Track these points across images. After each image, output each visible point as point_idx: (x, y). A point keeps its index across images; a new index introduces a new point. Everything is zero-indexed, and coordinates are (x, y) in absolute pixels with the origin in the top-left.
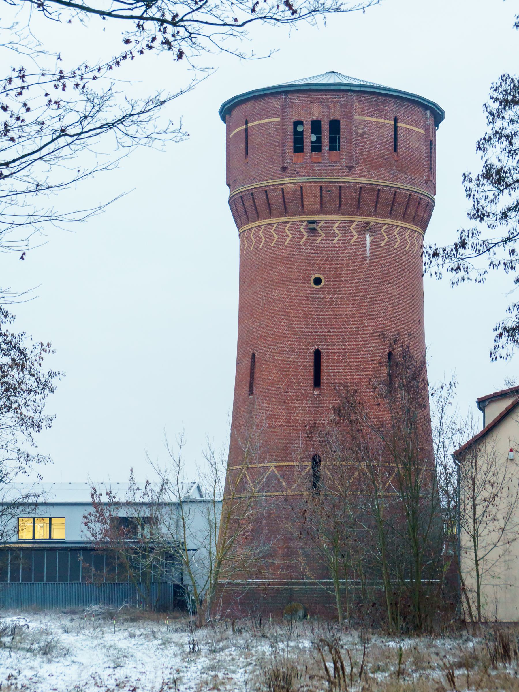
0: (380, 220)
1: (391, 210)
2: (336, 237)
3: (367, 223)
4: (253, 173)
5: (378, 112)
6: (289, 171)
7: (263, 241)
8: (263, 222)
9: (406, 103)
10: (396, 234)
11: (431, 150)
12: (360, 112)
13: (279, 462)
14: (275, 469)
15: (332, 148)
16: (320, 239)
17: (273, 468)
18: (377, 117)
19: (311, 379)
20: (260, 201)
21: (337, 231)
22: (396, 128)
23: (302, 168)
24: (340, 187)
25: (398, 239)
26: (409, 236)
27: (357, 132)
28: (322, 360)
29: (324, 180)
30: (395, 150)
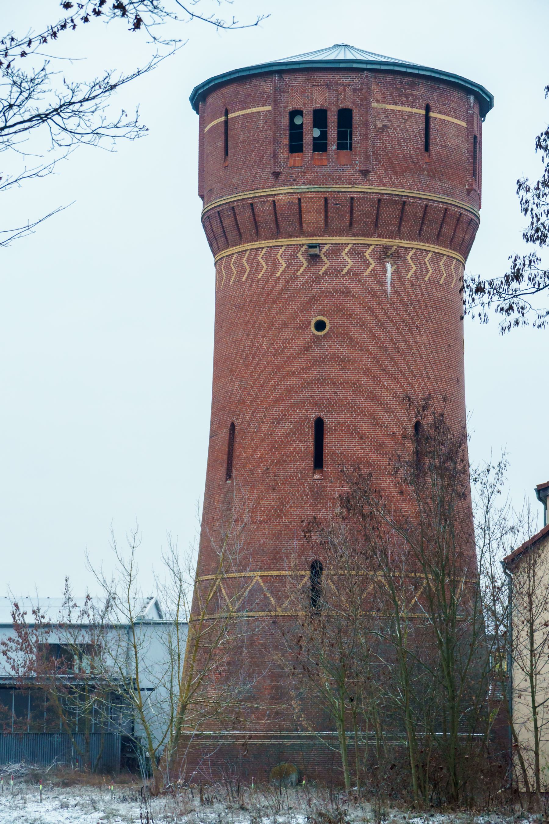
0: (405, 243)
1: (421, 230)
2: (345, 266)
3: (388, 248)
4: (234, 180)
5: (404, 99)
6: (283, 178)
7: (248, 271)
8: (248, 246)
9: (442, 86)
10: (427, 263)
11: (475, 148)
12: (379, 98)
13: (266, 570)
14: (260, 580)
15: (341, 146)
16: (324, 269)
17: (258, 578)
18: (402, 104)
19: (310, 458)
20: (244, 217)
21: (347, 258)
22: (427, 119)
23: (301, 173)
24: (352, 199)
25: (430, 269)
26: (445, 265)
27: (375, 125)
28: (325, 432)
29: (330, 190)
30: (427, 148)
